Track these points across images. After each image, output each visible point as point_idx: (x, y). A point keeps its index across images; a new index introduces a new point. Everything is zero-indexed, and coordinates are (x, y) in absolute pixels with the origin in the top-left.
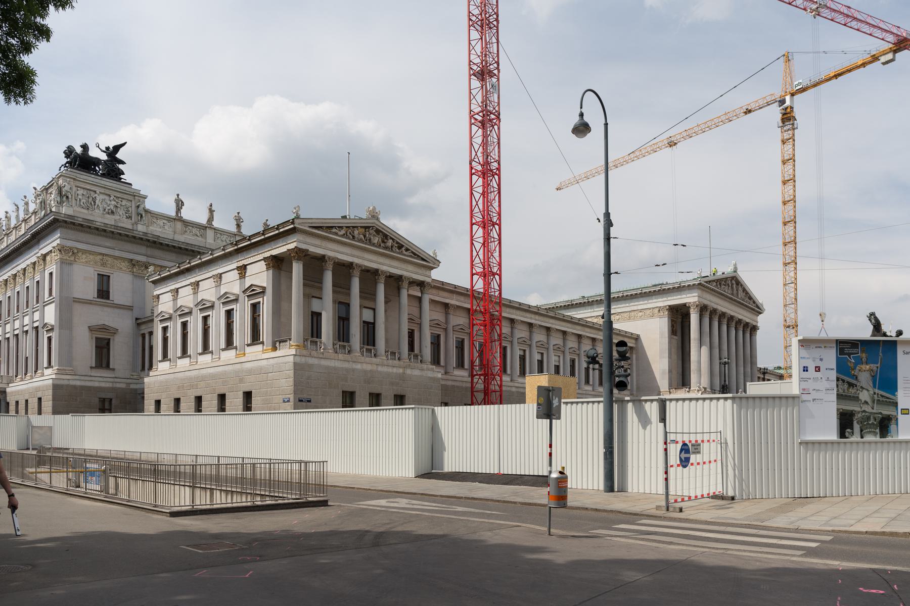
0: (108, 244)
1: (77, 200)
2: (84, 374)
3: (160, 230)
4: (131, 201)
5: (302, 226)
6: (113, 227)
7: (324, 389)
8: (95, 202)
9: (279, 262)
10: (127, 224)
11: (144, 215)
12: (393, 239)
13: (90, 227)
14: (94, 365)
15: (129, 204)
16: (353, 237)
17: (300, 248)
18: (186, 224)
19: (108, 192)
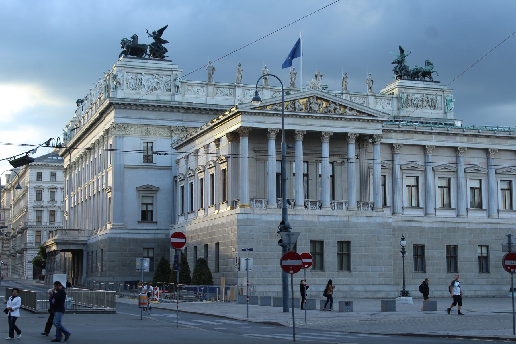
0: (151, 116)
1: (127, 84)
2: (133, 228)
3: (195, 96)
4: (170, 76)
5: (244, 109)
6: (154, 102)
7: (266, 240)
8: (141, 83)
9: (237, 137)
10: (166, 97)
11: (180, 87)
12: (335, 103)
13: (136, 105)
14: (140, 220)
15: (168, 79)
16: (295, 109)
17: (244, 127)
18: (218, 86)
19: (151, 72)
